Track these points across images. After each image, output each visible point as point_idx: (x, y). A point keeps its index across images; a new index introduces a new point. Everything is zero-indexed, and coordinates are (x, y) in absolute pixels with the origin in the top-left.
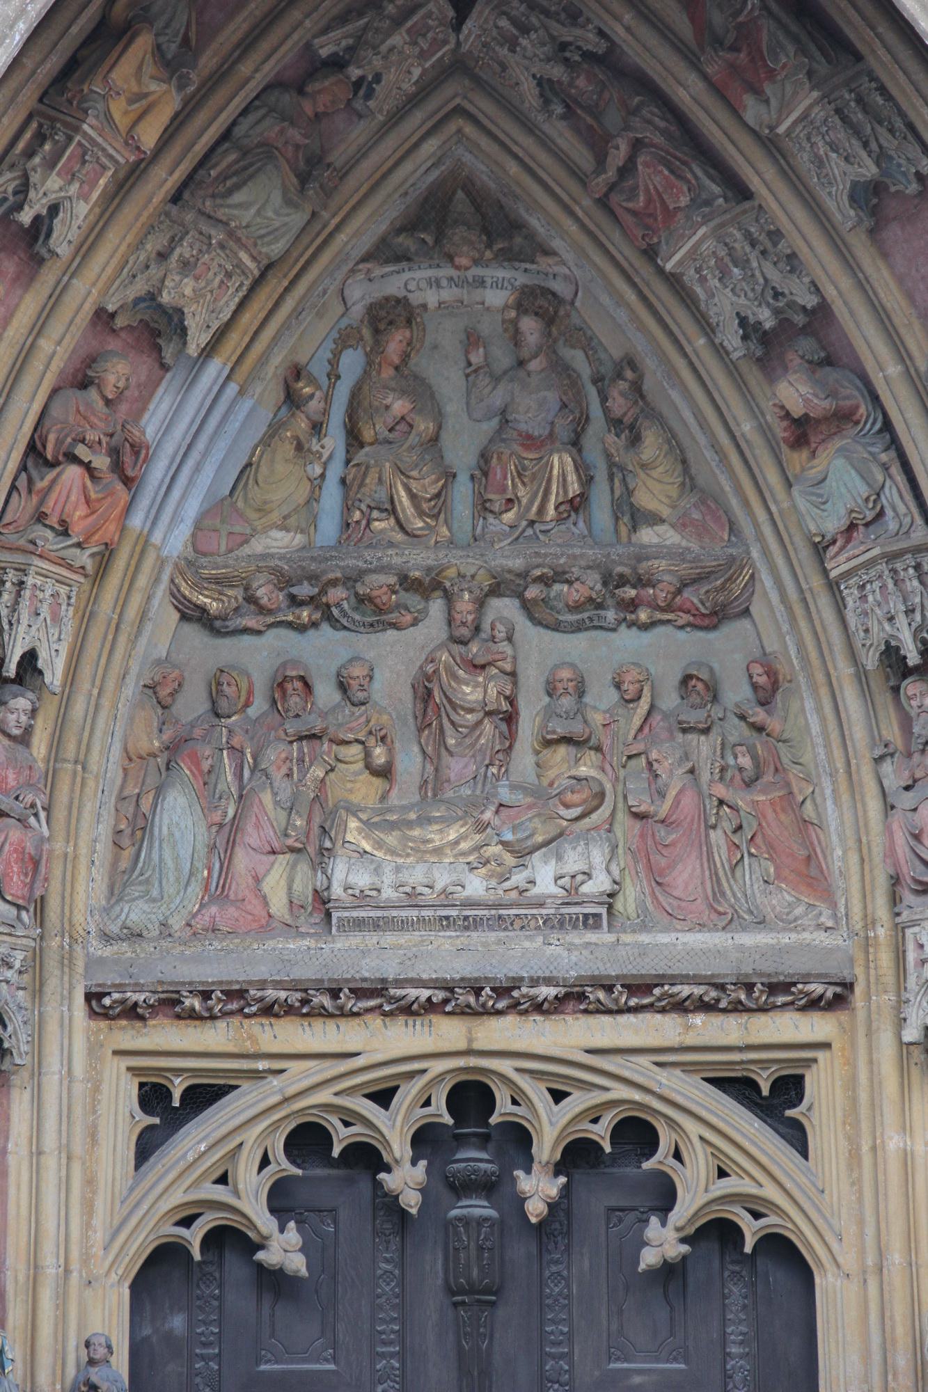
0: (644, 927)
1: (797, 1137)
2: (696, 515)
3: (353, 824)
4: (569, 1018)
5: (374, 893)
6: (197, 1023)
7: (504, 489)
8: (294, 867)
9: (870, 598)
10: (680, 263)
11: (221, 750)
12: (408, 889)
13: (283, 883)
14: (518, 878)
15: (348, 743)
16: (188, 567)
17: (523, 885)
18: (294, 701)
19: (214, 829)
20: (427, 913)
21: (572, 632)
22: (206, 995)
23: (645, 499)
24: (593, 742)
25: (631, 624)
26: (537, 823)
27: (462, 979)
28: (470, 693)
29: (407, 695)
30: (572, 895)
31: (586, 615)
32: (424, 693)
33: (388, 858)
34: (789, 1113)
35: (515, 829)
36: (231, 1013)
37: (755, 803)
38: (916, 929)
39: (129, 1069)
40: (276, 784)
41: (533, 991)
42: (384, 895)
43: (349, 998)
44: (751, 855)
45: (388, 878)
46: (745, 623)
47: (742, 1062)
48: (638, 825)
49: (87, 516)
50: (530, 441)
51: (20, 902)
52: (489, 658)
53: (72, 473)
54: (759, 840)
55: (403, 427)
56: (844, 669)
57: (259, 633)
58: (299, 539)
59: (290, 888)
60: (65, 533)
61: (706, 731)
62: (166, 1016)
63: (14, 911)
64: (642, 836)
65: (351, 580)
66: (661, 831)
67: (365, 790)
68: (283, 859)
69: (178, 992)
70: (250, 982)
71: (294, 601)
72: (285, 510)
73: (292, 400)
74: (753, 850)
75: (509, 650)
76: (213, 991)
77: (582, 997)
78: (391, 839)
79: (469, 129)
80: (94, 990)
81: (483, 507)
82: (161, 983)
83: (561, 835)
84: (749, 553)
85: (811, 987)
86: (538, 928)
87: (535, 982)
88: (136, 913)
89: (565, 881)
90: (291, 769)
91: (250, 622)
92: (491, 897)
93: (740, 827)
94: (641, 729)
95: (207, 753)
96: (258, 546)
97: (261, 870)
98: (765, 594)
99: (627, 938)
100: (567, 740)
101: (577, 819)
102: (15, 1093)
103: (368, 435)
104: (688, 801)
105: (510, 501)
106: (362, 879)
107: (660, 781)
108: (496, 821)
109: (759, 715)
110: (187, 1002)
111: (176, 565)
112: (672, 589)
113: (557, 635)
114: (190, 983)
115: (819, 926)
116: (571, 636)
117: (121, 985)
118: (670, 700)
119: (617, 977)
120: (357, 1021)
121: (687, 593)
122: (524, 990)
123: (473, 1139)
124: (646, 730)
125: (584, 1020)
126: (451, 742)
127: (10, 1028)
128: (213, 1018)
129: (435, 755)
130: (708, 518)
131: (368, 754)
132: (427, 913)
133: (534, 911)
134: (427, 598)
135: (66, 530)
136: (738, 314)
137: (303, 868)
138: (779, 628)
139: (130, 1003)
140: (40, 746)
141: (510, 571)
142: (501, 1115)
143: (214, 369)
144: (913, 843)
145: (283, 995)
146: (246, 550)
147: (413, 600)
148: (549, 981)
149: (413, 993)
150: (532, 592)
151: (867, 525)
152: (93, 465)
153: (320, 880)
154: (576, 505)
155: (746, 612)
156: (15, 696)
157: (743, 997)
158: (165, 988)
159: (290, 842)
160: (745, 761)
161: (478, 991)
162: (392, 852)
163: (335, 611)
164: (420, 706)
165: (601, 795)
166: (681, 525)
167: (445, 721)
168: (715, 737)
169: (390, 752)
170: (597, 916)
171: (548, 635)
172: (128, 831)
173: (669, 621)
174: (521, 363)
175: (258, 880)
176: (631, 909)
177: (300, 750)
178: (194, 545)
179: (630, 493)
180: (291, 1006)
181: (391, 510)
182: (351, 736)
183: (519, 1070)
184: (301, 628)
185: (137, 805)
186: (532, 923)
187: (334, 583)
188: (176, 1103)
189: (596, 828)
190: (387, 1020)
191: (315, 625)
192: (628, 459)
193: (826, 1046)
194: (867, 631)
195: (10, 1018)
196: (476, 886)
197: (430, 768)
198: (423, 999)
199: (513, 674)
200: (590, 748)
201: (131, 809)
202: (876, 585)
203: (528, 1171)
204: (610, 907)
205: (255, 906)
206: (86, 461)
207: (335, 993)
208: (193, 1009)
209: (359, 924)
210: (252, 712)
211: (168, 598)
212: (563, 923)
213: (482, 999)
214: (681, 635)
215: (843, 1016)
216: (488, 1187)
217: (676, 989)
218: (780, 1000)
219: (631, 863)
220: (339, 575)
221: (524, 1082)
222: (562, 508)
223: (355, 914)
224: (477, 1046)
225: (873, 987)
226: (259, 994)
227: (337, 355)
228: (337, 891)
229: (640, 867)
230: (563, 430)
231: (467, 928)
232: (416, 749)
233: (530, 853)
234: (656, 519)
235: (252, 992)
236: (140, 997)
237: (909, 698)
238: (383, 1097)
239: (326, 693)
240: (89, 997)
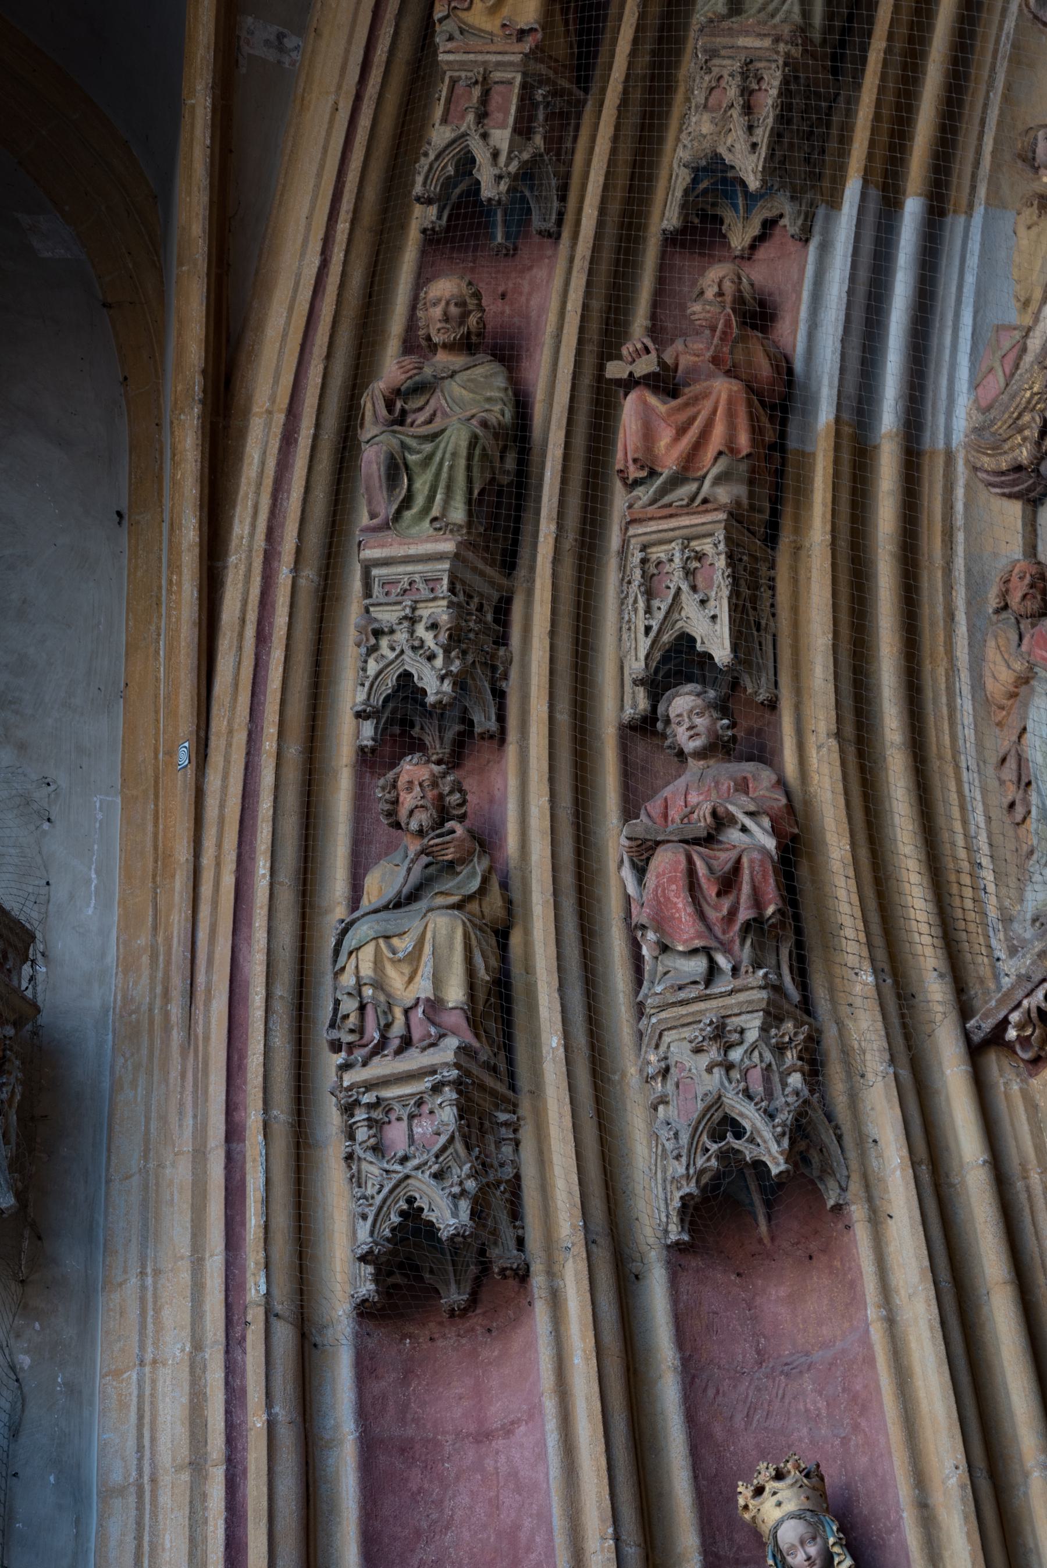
51: (698, 943)
139: (1034, 1014)
152: (637, 375)
195: (741, 1115)
206: (625, 376)
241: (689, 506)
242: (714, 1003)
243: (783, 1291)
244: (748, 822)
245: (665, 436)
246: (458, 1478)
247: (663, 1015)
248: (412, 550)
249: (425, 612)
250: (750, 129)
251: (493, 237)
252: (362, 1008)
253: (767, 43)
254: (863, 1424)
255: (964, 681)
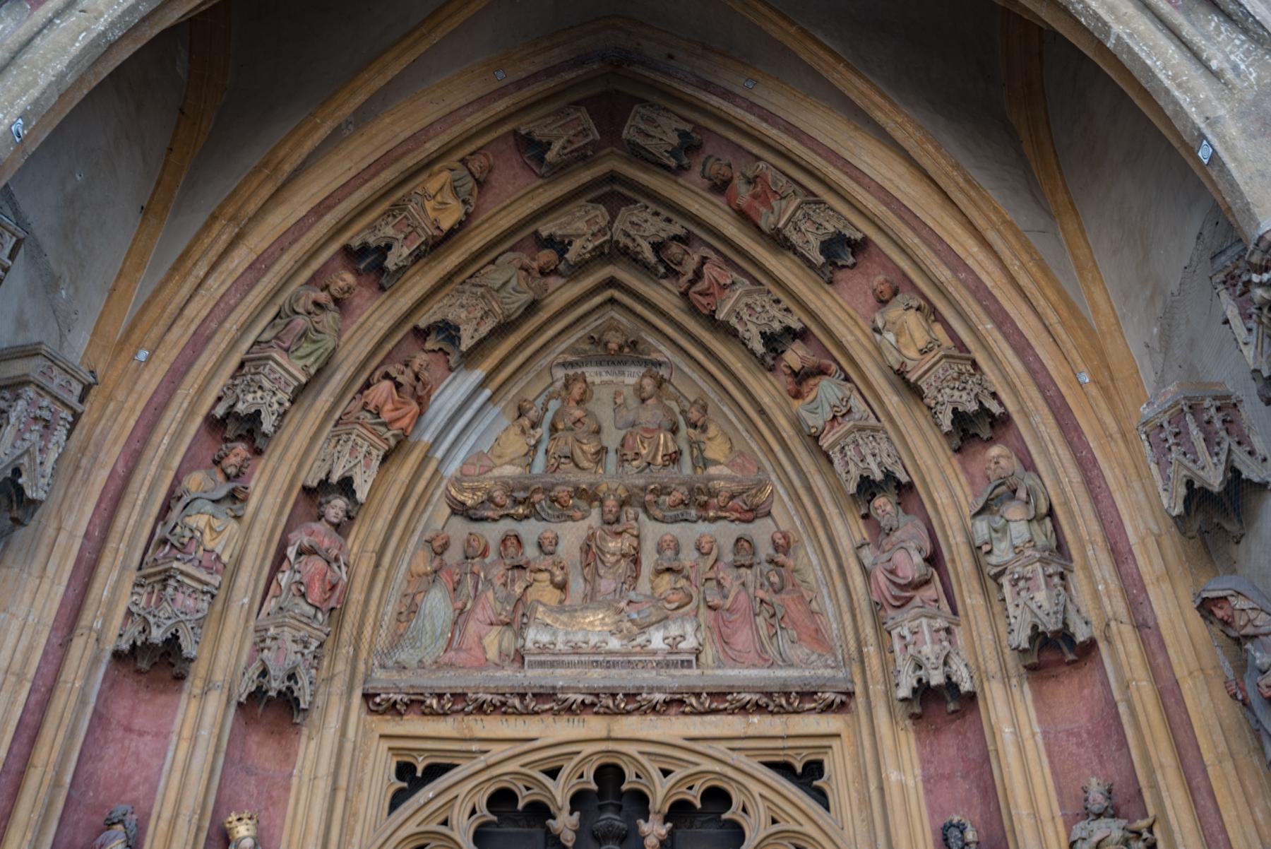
0: (719, 667)
1: (821, 797)
2: (739, 461)
3: (541, 609)
4: (673, 719)
5: (552, 646)
6: (435, 718)
7: (633, 448)
8: (504, 633)
9: (849, 453)
10: (728, 314)
11: (466, 574)
12: (573, 644)
13: (496, 642)
14: (641, 640)
15: (540, 570)
16: (458, 481)
17: (643, 643)
18: (512, 550)
19: (457, 612)
20: (583, 658)
21: (672, 523)
22: (440, 696)
23: (709, 454)
24: (685, 572)
25: (704, 520)
26: (653, 610)
27: (604, 687)
28: (613, 545)
29: (577, 554)
30: (673, 649)
31: (679, 512)
32: (586, 549)
33: (561, 627)
34: (816, 783)
35: (638, 613)
36: (457, 712)
37: (782, 600)
38: (899, 629)
39: (390, 749)
40: (496, 588)
41: (649, 697)
42: (558, 647)
43: (532, 700)
44: (782, 628)
45: (561, 639)
46: (768, 521)
47: (783, 749)
48: (713, 613)
49: (392, 410)
50: (646, 430)
51: (318, 604)
52: (625, 527)
53: (387, 385)
54: (786, 619)
55: (579, 425)
56: (831, 510)
57: (494, 520)
58: (518, 470)
59: (500, 646)
60: (378, 415)
61: (750, 566)
62: (415, 713)
63: (311, 611)
64: (716, 619)
65: (546, 490)
66: (726, 615)
67: (551, 596)
68: (496, 629)
69: (422, 694)
70: (468, 688)
71: (517, 502)
72: (513, 456)
73: (521, 413)
74: (783, 625)
75: (635, 524)
76: (445, 694)
77: (681, 702)
78: (564, 618)
79: (617, 294)
80: (371, 691)
81: (623, 460)
82: (412, 687)
83: (666, 618)
84: (769, 478)
85: (827, 695)
86: (653, 668)
87: (651, 690)
88: (403, 656)
89: (670, 641)
90: (506, 582)
91: (490, 514)
92: (624, 651)
93: (773, 615)
94: (712, 567)
95: (457, 571)
96: (496, 472)
97: (483, 633)
98: (780, 497)
99: (709, 672)
100: (669, 570)
101: (678, 608)
102: (304, 739)
103: (560, 426)
104: (743, 598)
105: (637, 454)
106: (545, 638)
107: (725, 590)
108: (627, 609)
109: (780, 558)
110: (428, 702)
111: (450, 480)
112: (728, 495)
113: (664, 525)
114: (431, 687)
115: (827, 666)
116: (670, 526)
117: (386, 688)
118: (729, 557)
119: (703, 688)
120: (537, 718)
121: (735, 501)
122: (644, 695)
123: (611, 808)
124: (715, 568)
125: (682, 719)
126: (602, 572)
127: (300, 685)
128: (445, 714)
129: (592, 580)
130: (746, 463)
131: (552, 574)
132: (583, 658)
133: (651, 658)
134: (590, 505)
135: (378, 414)
136: (761, 333)
137: (509, 635)
138: (789, 513)
139: (392, 701)
140: (353, 542)
141: (636, 487)
142: (629, 782)
143: (477, 374)
144: (892, 577)
145: (489, 697)
146: (490, 474)
147: (583, 505)
148: (660, 689)
149: (572, 697)
150: (649, 497)
151: (843, 416)
153: (520, 642)
154: (674, 458)
155: (769, 514)
156: (336, 498)
157: (784, 702)
158: (416, 691)
159: (502, 617)
160: (775, 579)
161: (614, 696)
162: (565, 624)
163: (538, 507)
164: (584, 556)
165: (691, 597)
166: (730, 465)
167: (598, 562)
168: (757, 569)
169: (566, 574)
170: (689, 662)
171: (659, 525)
172: (405, 613)
173: (725, 518)
174: (643, 401)
175: (480, 638)
176: (710, 661)
177: (513, 575)
178: (461, 471)
179: (701, 451)
180: (495, 706)
181: (570, 457)
182: (543, 567)
183: (642, 753)
184: (521, 518)
185: (413, 599)
186: (650, 665)
187: (536, 491)
188: (419, 774)
189: (687, 614)
190: (557, 718)
191: (527, 517)
192: (703, 437)
193: (838, 736)
194: (848, 472)
196: (615, 644)
197: (589, 587)
198: (579, 701)
199: (637, 537)
200: (683, 577)
201: (409, 601)
202: (852, 447)
203: (647, 820)
204: (697, 659)
205: (477, 652)
207: (522, 696)
208: (431, 707)
209: (542, 664)
210: (487, 560)
211: (444, 499)
212: (668, 665)
213: (617, 702)
214: (733, 526)
215: (848, 717)
216: (622, 838)
217: (742, 696)
218: (807, 706)
219: (709, 635)
220: (540, 485)
221: (644, 760)
222: (665, 458)
223: (538, 658)
224: (614, 735)
225: (869, 681)
226: (474, 696)
227: (547, 401)
228: (529, 644)
229: (716, 637)
230: (667, 424)
231: (609, 668)
232: (581, 581)
233: (648, 626)
234: (716, 463)
235: (470, 695)
236: (398, 697)
237: (876, 509)
238: (553, 773)
239: (531, 552)
240: (367, 697)
241: (379, 437)
242: (309, 629)
243: (257, 739)
244: (343, 566)
245: (389, 406)
246: (112, 741)
247: (292, 621)
248: (287, 366)
249: (280, 395)
250: (476, 330)
251: (359, 263)
252: (191, 538)
253: (500, 311)
254: (271, 809)
255: (407, 558)
